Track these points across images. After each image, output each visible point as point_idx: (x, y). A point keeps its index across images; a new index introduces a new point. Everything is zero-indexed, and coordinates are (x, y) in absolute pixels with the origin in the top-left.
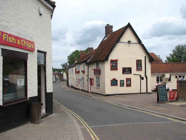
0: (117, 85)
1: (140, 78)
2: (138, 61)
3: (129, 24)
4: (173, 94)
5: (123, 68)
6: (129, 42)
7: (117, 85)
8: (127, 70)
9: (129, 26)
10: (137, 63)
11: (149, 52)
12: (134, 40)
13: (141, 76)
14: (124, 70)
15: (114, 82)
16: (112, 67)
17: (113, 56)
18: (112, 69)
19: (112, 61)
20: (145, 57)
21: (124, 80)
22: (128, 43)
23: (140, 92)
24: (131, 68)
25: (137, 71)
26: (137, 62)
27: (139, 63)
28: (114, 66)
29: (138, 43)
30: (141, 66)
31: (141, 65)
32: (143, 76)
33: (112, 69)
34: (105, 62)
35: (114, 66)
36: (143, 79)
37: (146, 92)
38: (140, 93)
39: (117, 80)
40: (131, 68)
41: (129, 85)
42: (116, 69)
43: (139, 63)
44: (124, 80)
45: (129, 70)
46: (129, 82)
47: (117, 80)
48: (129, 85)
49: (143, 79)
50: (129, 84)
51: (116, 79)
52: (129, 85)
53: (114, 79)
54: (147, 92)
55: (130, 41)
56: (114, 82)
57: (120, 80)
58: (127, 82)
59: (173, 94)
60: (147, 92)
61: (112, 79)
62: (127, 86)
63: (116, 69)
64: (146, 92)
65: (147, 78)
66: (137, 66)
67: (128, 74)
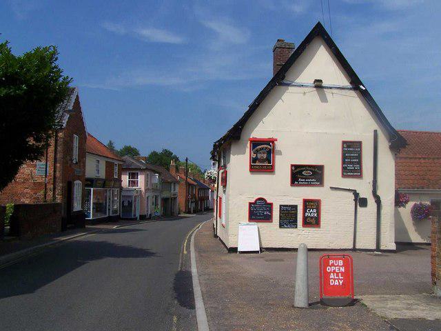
0: (268, 218)
1: (355, 200)
2: (348, 147)
3: (319, 25)
4: (342, 269)
5: (292, 166)
6: (318, 85)
7: (268, 218)
8: (304, 174)
9: (319, 34)
10: (343, 150)
11: (271, 76)
12: (333, 75)
13: (356, 194)
14: (297, 173)
15: (259, 211)
16: (254, 160)
17: (261, 130)
18: (253, 169)
19: (255, 143)
20: (375, 132)
21: (296, 207)
22: (316, 87)
23: (351, 247)
24: (321, 168)
25: (343, 176)
26: (343, 147)
27: (351, 152)
28: (263, 158)
29: (351, 89)
30: (360, 163)
31: (359, 157)
32: (365, 192)
33: (253, 169)
34: (233, 149)
35: (263, 158)
36: (363, 202)
37: (374, 247)
38: (354, 249)
39: (271, 204)
40: (321, 168)
41: (313, 221)
42: (270, 169)
43: (351, 152)
44: (296, 207)
45: (314, 173)
46: (312, 213)
47: (271, 204)
48: (313, 222)
49: (363, 202)
50: (312, 218)
51: (268, 201)
52: (313, 222)
53: (260, 199)
54: (378, 249)
55: (321, 81)
56: (259, 211)
57: (281, 206)
58: (305, 211)
59: (342, 269)
60: (378, 249)
61: (253, 201)
62: (307, 223)
63: (270, 169)
64: (374, 247)
65: (378, 201)
66: (344, 162)
67: (310, 185)
